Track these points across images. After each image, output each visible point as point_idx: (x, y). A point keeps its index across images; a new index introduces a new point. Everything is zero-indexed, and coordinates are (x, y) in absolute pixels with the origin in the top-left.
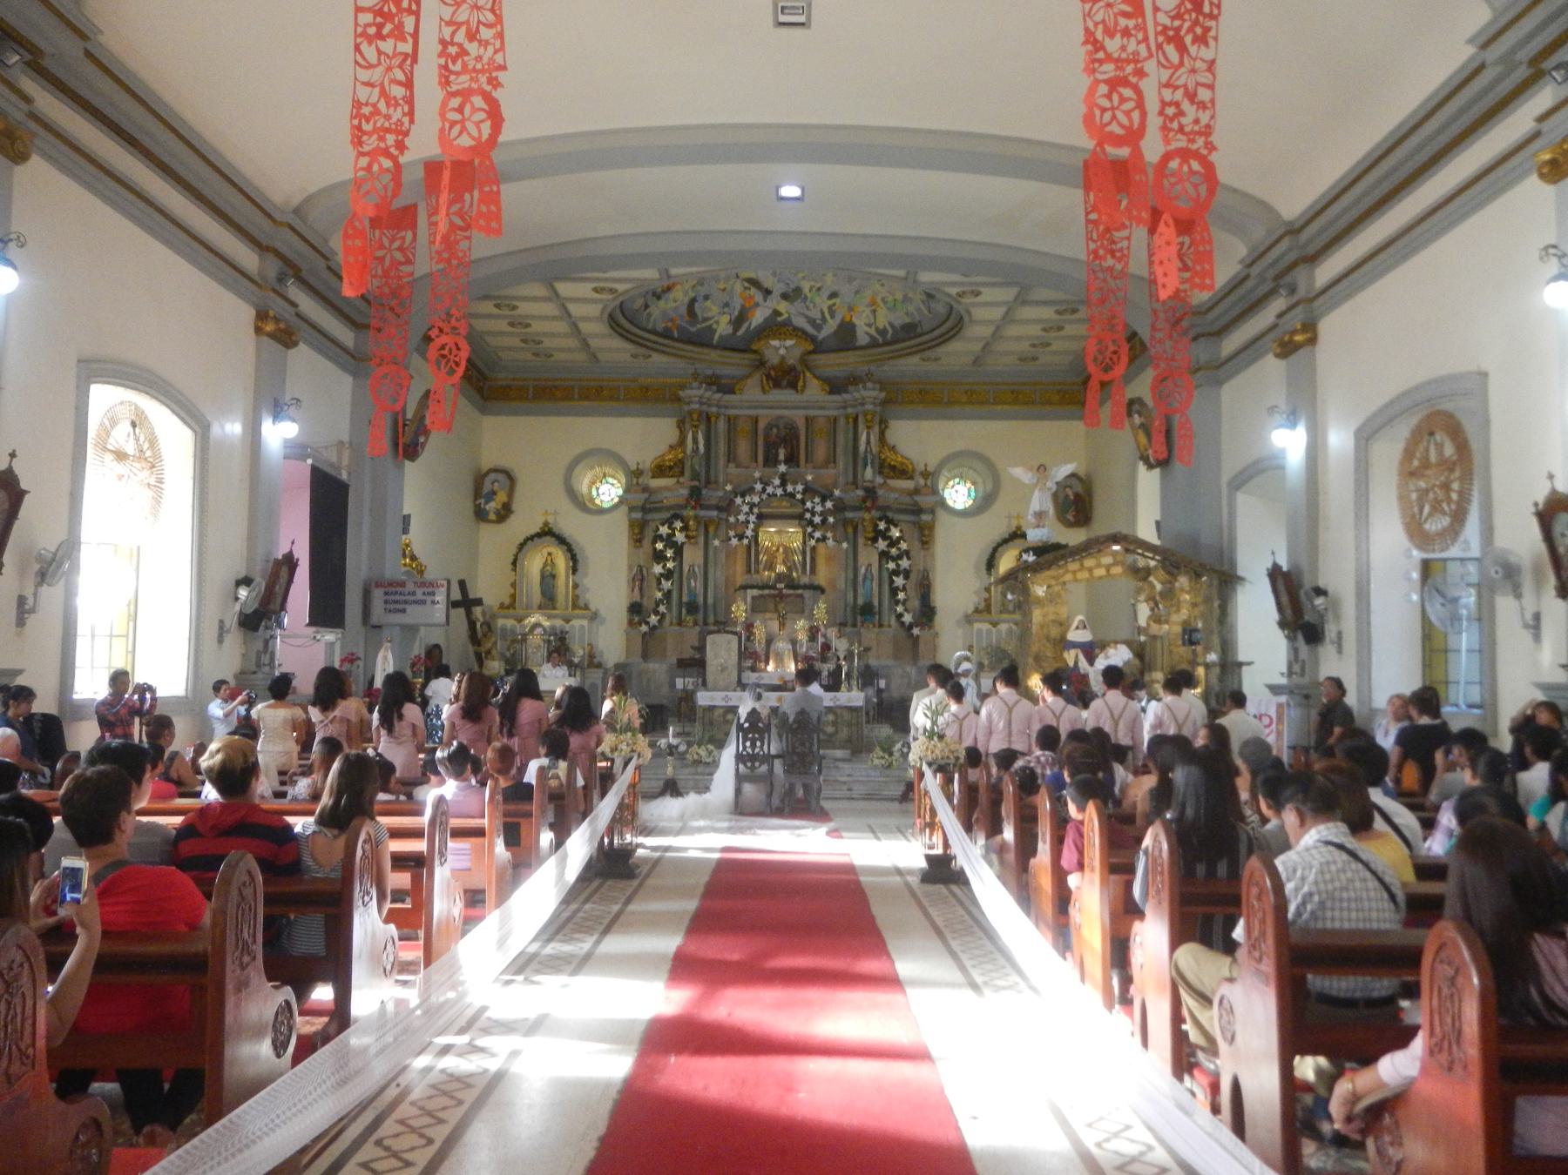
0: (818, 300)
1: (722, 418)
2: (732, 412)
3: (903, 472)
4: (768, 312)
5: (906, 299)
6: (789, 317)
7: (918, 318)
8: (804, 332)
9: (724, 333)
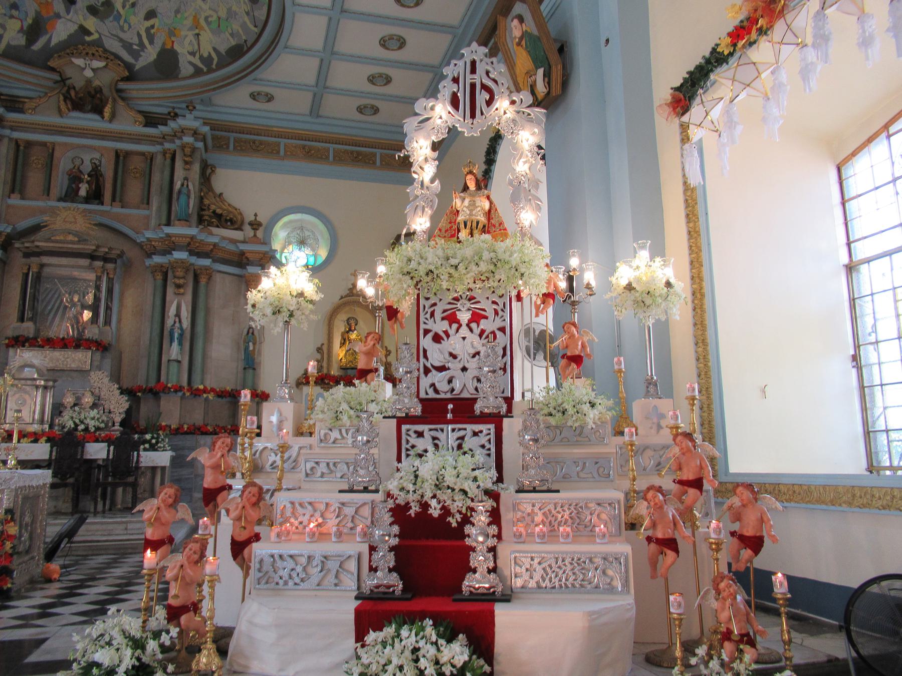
0: (133, 20)
1: (6, 141)
2: (16, 135)
3: (230, 220)
4: (73, 28)
5: (231, 14)
6: (100, 39)
7: (244, 38)
8: (117, 57)
9: (12, 43)
